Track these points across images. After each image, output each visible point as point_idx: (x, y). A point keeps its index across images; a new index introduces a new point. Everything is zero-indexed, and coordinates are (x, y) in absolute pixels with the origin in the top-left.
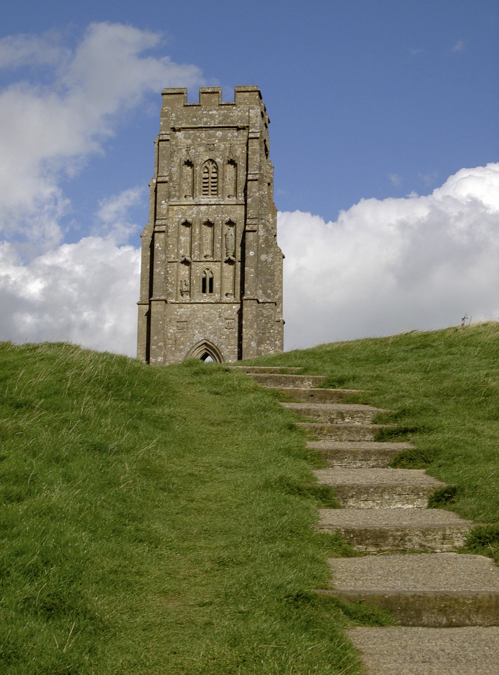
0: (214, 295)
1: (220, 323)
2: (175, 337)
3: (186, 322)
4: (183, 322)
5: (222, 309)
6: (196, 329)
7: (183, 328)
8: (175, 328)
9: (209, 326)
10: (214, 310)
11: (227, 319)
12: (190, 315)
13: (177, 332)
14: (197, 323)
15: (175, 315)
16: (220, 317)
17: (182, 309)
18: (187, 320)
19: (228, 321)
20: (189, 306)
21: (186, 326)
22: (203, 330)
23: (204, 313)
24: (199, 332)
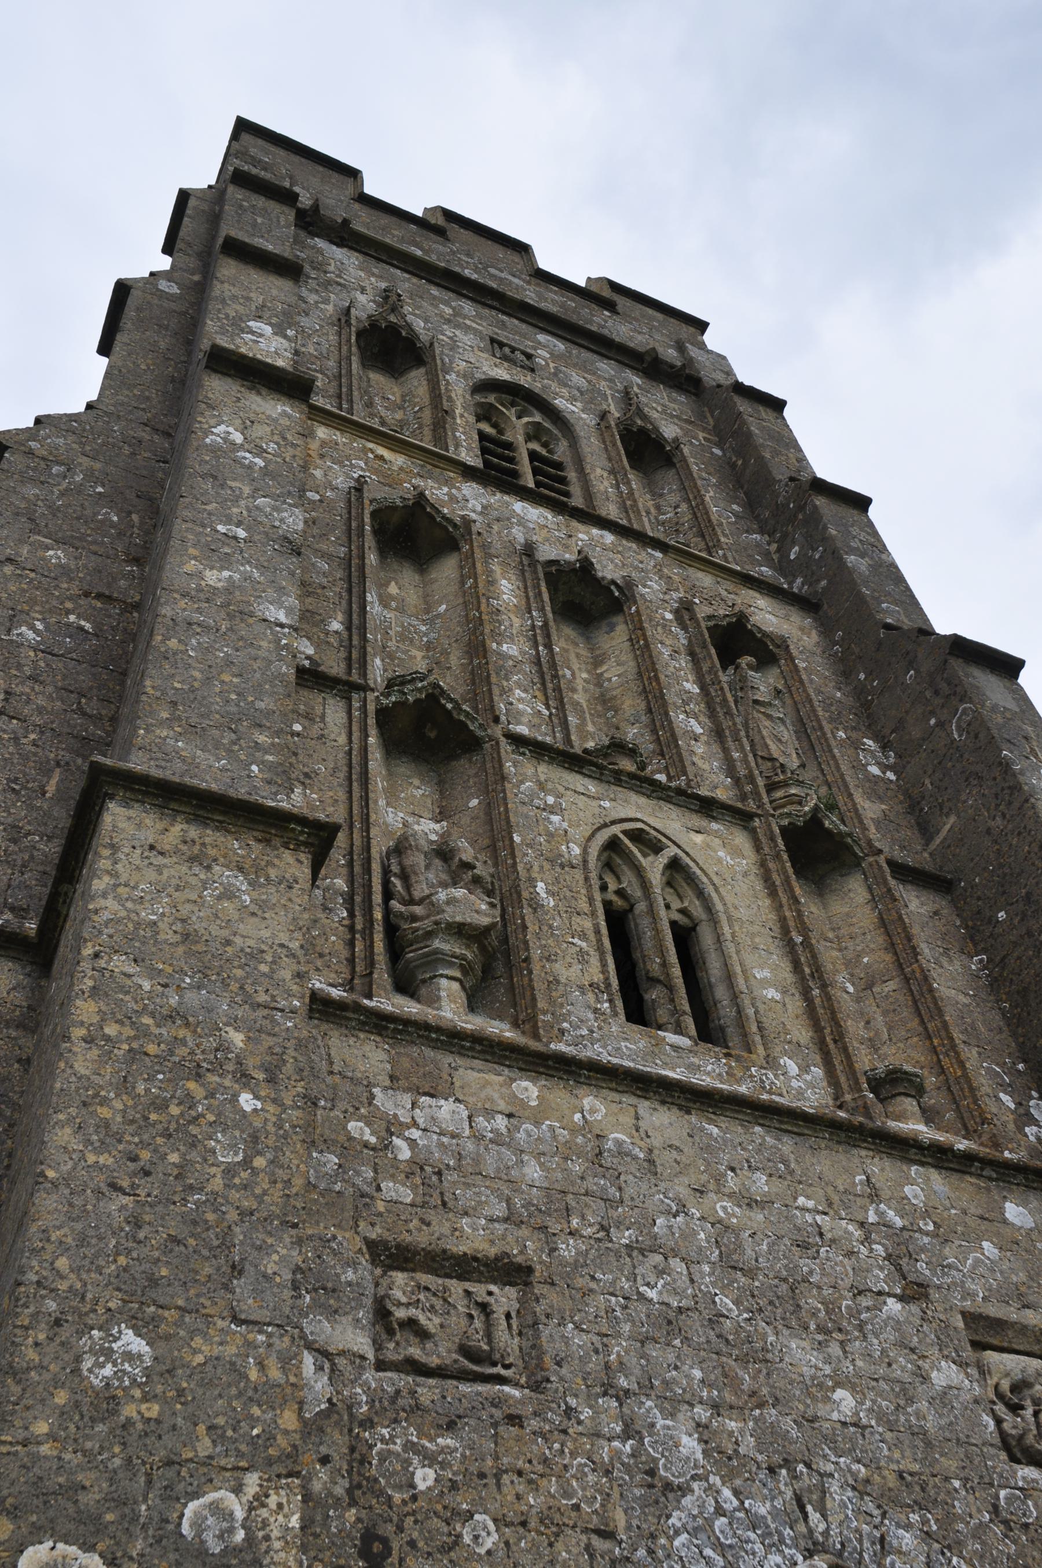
0: (771, 1063)
1: (945, 1374)
2: (361, 1486)
3: (513, 1272)
4: (464, 1267)
5: (902, 1204)
6: (671, 1405)
7: (477, 1363)
8: (354, 1337)
9: (819, 1389)
10: (828, 1207)
11: (985, 1333)
12: (560, 1201)
13: (390, 1409)
14: (670, 1322)
15: (348, 1148)
16: (915, 1292)
17: (446, 1110)
18: (528, 1248)
19: (1006, 1365)
20: (529, 1090)
21: (507, 1341)
22: (768, 1435)
23: (723, 1207)
24: (723, 1458)
